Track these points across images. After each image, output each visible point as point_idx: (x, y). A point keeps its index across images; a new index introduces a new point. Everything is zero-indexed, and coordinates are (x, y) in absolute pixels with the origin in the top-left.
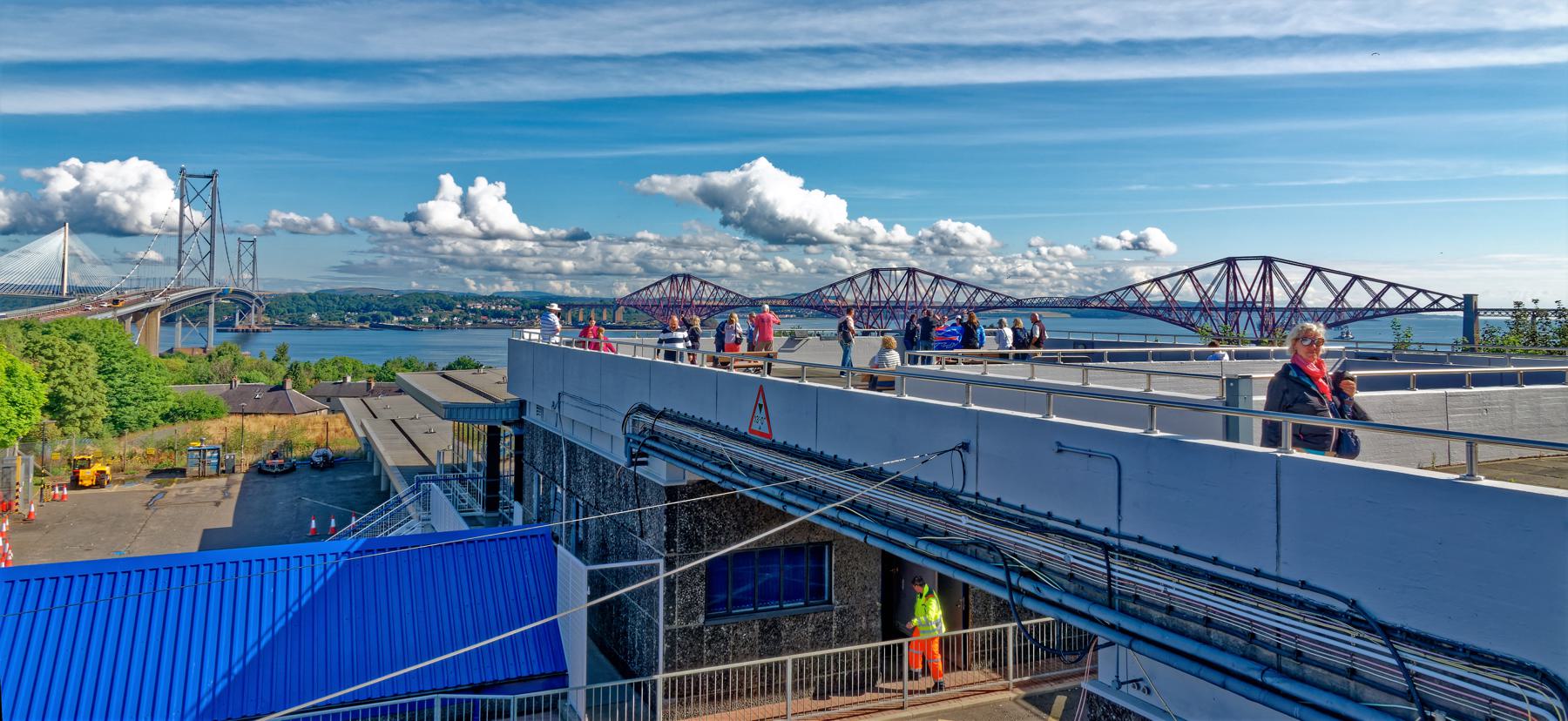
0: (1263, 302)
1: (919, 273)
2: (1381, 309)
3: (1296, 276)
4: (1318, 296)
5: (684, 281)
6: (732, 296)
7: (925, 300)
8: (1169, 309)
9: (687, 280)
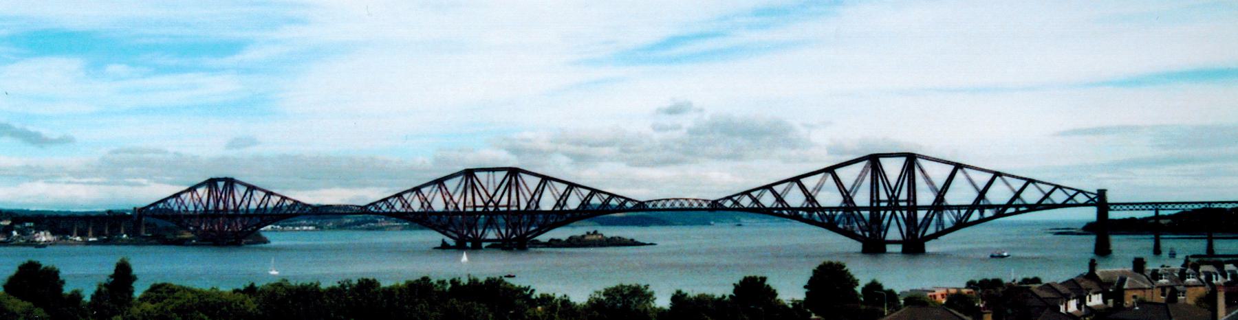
0: (908, 201)
1: (521, 174)
3: (939, 173)
4: (961, 194)
5: (225, 187)
6: (288, 203)
7: (531, 204)
8: (810, 211)
9: (229, 183)
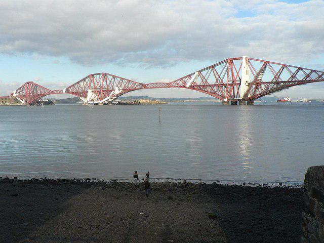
2: (295, 81)
7: (109, 87)
